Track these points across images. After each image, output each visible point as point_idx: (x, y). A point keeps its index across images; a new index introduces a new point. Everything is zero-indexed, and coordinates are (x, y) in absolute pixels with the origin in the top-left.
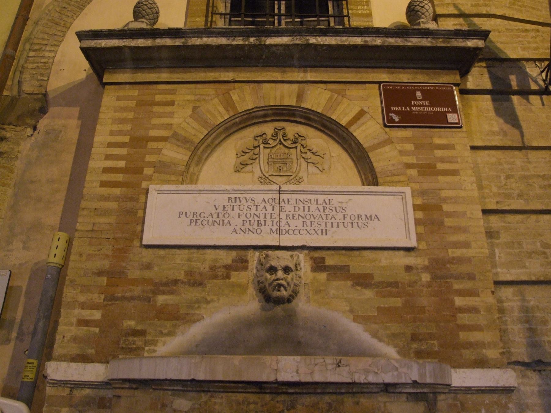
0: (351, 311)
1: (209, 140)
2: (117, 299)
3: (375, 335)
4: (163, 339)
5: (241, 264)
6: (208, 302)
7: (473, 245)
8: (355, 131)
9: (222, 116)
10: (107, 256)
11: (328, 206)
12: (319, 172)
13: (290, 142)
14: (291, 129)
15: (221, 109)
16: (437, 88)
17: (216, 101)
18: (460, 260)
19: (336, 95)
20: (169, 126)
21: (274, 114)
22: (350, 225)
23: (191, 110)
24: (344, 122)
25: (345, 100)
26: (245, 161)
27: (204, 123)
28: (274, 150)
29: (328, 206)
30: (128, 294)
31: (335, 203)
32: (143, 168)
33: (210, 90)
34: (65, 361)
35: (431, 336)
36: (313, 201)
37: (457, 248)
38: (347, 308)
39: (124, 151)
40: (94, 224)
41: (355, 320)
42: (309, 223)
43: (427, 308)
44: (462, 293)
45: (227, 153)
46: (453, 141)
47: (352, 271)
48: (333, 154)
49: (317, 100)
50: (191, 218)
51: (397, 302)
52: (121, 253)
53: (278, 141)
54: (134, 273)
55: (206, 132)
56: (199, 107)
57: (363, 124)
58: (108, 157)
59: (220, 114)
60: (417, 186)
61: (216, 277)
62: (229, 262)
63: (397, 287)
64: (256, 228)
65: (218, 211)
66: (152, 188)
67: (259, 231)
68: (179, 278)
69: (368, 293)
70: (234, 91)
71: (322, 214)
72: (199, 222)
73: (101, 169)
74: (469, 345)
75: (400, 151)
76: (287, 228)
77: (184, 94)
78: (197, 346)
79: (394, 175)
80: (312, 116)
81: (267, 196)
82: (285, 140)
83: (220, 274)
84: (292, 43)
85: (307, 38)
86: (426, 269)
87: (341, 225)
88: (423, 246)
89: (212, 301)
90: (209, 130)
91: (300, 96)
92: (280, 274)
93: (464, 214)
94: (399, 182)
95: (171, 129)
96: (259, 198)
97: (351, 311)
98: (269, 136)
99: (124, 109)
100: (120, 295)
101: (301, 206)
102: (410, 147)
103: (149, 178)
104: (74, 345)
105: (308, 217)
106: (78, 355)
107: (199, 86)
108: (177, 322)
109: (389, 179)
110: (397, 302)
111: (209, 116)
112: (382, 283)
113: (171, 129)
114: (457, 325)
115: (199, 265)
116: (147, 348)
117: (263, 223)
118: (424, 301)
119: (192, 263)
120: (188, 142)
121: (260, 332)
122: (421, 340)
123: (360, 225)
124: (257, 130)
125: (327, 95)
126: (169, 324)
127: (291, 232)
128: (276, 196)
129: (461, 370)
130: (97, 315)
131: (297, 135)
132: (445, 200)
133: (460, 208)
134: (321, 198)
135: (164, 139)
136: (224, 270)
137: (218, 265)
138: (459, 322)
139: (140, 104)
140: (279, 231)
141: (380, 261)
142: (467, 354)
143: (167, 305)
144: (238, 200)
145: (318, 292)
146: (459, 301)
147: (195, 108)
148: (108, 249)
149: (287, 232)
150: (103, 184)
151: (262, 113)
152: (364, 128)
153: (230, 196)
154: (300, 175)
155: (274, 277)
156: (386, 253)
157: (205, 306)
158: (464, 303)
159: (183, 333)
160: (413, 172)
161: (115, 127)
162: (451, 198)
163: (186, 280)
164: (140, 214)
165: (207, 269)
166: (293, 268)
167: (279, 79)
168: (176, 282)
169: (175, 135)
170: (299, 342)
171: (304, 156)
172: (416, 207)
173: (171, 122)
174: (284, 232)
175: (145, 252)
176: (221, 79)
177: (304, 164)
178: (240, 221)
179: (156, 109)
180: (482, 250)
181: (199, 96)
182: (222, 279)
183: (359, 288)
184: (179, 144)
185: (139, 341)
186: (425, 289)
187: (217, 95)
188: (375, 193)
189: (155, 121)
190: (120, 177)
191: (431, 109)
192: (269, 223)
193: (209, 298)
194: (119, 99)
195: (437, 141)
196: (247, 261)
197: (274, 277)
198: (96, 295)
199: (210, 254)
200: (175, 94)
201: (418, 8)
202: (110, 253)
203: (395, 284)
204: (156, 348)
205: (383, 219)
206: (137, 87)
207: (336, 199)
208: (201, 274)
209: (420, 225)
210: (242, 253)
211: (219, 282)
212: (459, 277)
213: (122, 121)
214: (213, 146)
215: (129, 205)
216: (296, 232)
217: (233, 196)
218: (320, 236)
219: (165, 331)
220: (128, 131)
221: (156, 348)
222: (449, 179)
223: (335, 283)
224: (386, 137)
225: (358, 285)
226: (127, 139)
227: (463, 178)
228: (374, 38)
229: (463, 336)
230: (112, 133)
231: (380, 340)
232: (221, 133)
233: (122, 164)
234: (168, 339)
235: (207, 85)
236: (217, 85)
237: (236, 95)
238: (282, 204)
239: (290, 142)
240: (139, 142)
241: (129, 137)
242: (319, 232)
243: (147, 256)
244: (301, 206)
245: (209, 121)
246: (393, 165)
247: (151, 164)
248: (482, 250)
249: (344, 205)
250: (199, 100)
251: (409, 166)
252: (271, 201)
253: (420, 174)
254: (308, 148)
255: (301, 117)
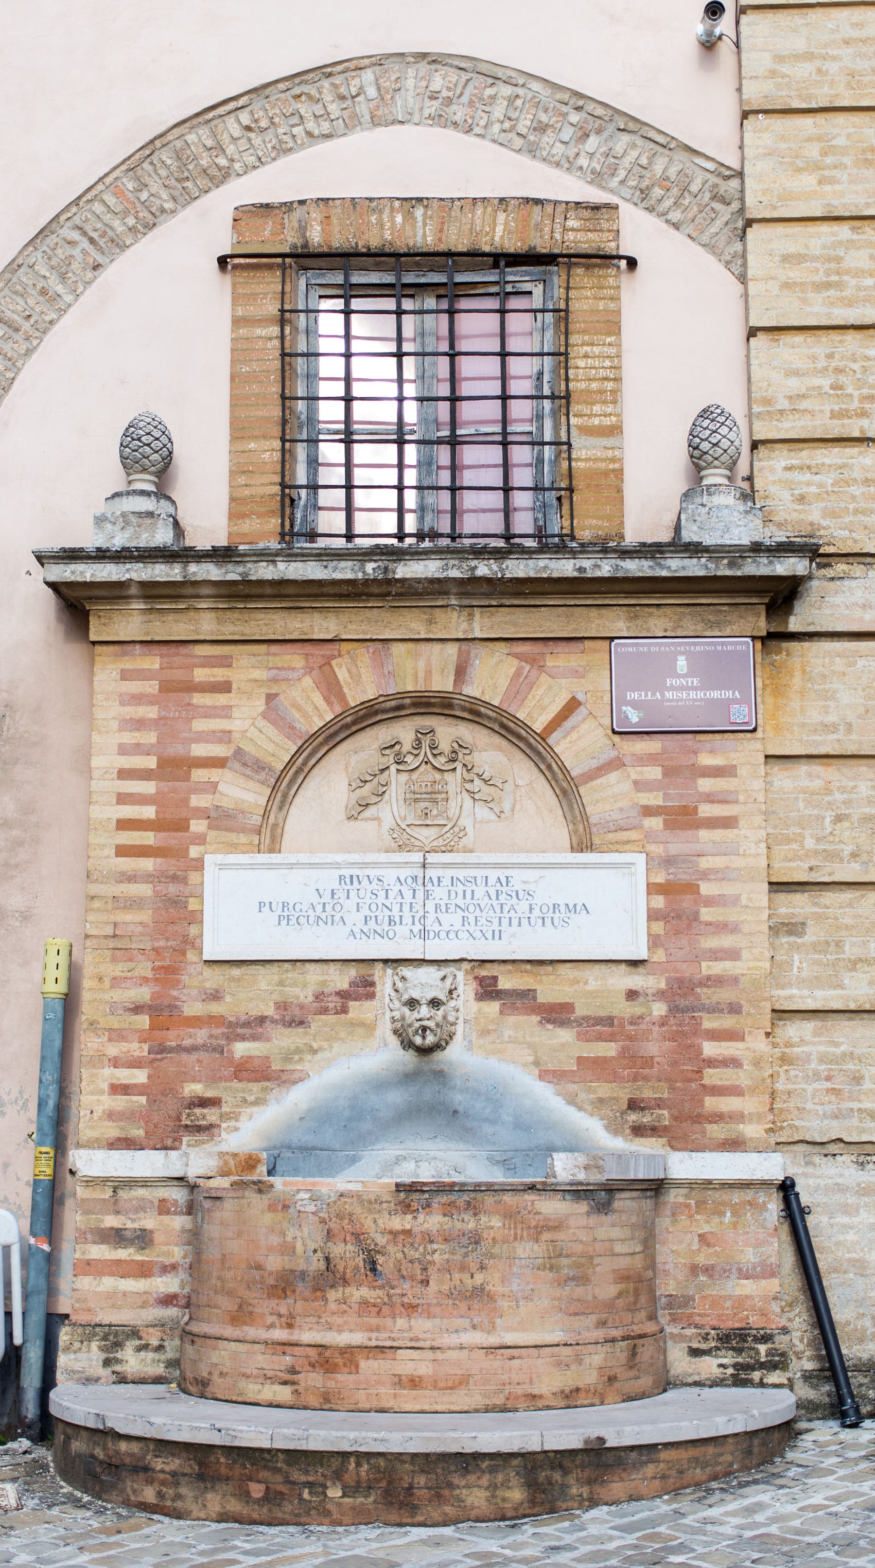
0: (536, 1063)
1: (300, 760)
2: (171, 1050)
3: (571, 1100)
4: (248, 1110)
5: (364, 988)
6: (315, 1052)
7: (745, 954)
8: (557, 743)
9: (321, 716)
10: (145, 980)
11: (504, 889)
12: (493, 817)
13: (443, 759)
14: (447, 732)
15: (318, 698)
16: (719, 648)
17: (308, 681)
18: (718, 981)
19: (527, 667)
20: (225, 737)
21: (414, 705)
22: (540, 921)
23: (263, 701)
24: (538, 727)
25: (544, 677)
26: (363, 798)
27: (289, 729)
28: (415, 776)
29: (504, 889)
30: (187, 1042)
31: (517, 883)
32: (187, 821)
33: (293, 658)
34: (99, 1148)
35: (660, 1104)
36: (479, 880)
37: (716, 959)
38: (531, 1059)
39: (149, 787)
40: (115, 925)
41: (541, 1077)
42: (472, 920)
43: (657, 1059)
44: (716, 1036)
45: (331, 784)
46: (734, 758)
47: (541, 999)
48: (519, 782)
49: (491, 678)
50: (279, 912)
51: (609, 1049)
52: (168, 974)
53: (421, 757)
54: (193, 1008)
55: (294, 749)
56: (277, 695)
57: (573, 728)
58: (123, 799)
59: (317, 713)
60: (656, 849)
61: (324, 1011)
62: (346, 986)
63: (612, 1025)
64: (387, 928)
65: (323, 900)
66: (208, 859)
67: (391, 934)
68: (266, 1014)
69: (565, 1035)
70: (339, 660)
71: (495, 902)
72: (293, 921)
73: (114, 823)
74: (718, 1117)
75: (636, 783)
76: (437, 928)
77: (248, 669)
78: (301, 1119)
79: (622, 829)
80: (482, 710)
81: (404, 873)
82: (435, 755)
83: (331, 1005)
84: (445, 574)
85: (473, 563)
86: (661, 995)
87: (524, 922)
88: (660, 956)
89: (321, 1049)
90: (299, 743)
91: (461, 672)
92: (424, 1011)
93: (736, 899)
94: (628, 842)
95: (230, 742)
96: (390, 875)
97: (536, 1063)
98: (407, 746)
99: (138, 699)
100: (174, 1044)
101: (460, 888)
102: (654, 773)
103: (201, 840)
104: (110, 1124)
105: (471, 908)
106: (119, 1139)
107: (274, 648)
108: (268, 1084)
109: (611, 836)
110: (609, 1049)
111: (297, 715)
112: (586, 1018)
113: (230, 742)
114: (704, 1086)
115: (297, 990)
116: (224, 1125)
117: (397, 920)
118: (654, 1048)
119: (287, 989)
120: (264, 769)
121: (397, 1097)
122: (642, 1109)
123: (556, 922)
124: (383, 734)
125: (510, 666)
126: (255, 1087)
127: (443, 935)
128: (419, 872)
129: (700, 1154)
130: (140, 1076)
131: (455, 745)
132: (705, 875)
133: (728, 889)
134: (493, 875)
135: (219, 763)
136: (337, 999)
137: (327, 991)
138: (706, 1081)
139: (167, 687)
140: (424, 934)
141: (586, 983)
142: (715, 1131)
143: (250, 1057)
144: (355, 879)
145: (484, 1033)
146: (710, 1049)
147: (270, 698)
148: (144, 968)
149: (437, 935)
150: (122, 851)
151: (393, 703)
152: (574, 736)
153: (344, 872)
154: (461, 823)
155: (416, 1015)
156: (597, 969)
157: (309, 1057)
158: (719, 1051)
159: (278, 1101)
160: (655, 823)
161: (128, 738)
162: (716, 871)
163: (277, 1017)
164: (193, 905)
165: (311, 999)
166: (444, 999)
167: (423, 636)
168: (262, 1020)
169: (239, 753)
170: (455, 1112)
171: (468, 786)
172: (653, 889)
173: (228, 728)
174: (432, 935)
175: (208, 972)
176: (315, 637)
177: (468, 802)
178: (360, 917)
179: (198, 699)
180: (759, 964)
181: (274, 672)
182: (337, 1013)
183: (550, 1026)
184: (248, 772)
185: (211, 1115)
186: (656, 1029)
187: (309, 670)
188: (585, 866)
189: (200, 725)
190: (148, 838)
191: (700, 695)
192: (407, 919)
193: (315, 1046)
194: (125, 676)
195: (706, 760)
196: (372, 984)
197: (416, 1015)
198: (135, 1045)
199: (314, 974)
200: (230, 666)
201: (705, 446)
202: (150, 974)
203: (609, 1021)
204: (238, 1124)
205: (596, 910)
206: (155, 649)
207: (518, 877)
208: (302, 1007)
209: (657, 919)
210: (364, 970)
211: (331, 1018)
212: (715, 1009)
213: (139, 724)
214: (306, 770)
215: (172, 889)
216: (452, 935)
217: (347, 872)
218: (490, 941)
219: (251, 1098)
220: (153, 746)
221: (238, 1124)
222: (718, 834)
223: (512, 1019)
224: (613, 754)
225: (549, 1021)
226: (151, 762)
227: (743, 832)
228: (599, 562)
229: (711, 1103)
230: (123, 750)
231: (580, 1109)
232: (321, 744)
233: (149, 812)
234: (255, 1109)
235: (289, 646)
236: (308, 648)
237: (344, 669)
238: (429, 886)
239: (443, 759)
240: (174, 767)
241: (155, 758)
242: (489, 935)
243: (213, 978)
244: (460, 888)
245: (297, 725)
246: (621, 810)
247: (203, 813)
248: (759, 964)
249: (531, 887)
250: (275, 680)
251: (648, 811)
252: (410, 880)
253: (669, 825)
254: (475, 770)
255: (464, 709)
